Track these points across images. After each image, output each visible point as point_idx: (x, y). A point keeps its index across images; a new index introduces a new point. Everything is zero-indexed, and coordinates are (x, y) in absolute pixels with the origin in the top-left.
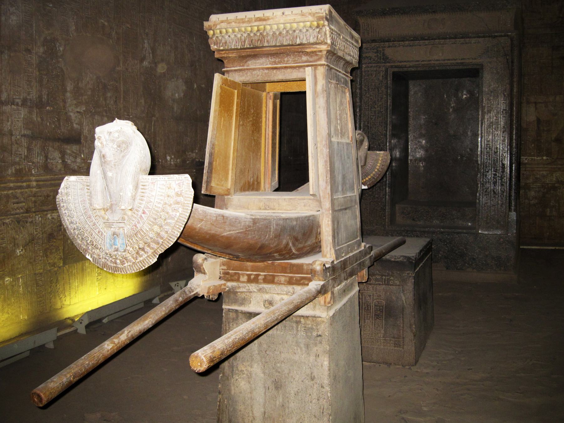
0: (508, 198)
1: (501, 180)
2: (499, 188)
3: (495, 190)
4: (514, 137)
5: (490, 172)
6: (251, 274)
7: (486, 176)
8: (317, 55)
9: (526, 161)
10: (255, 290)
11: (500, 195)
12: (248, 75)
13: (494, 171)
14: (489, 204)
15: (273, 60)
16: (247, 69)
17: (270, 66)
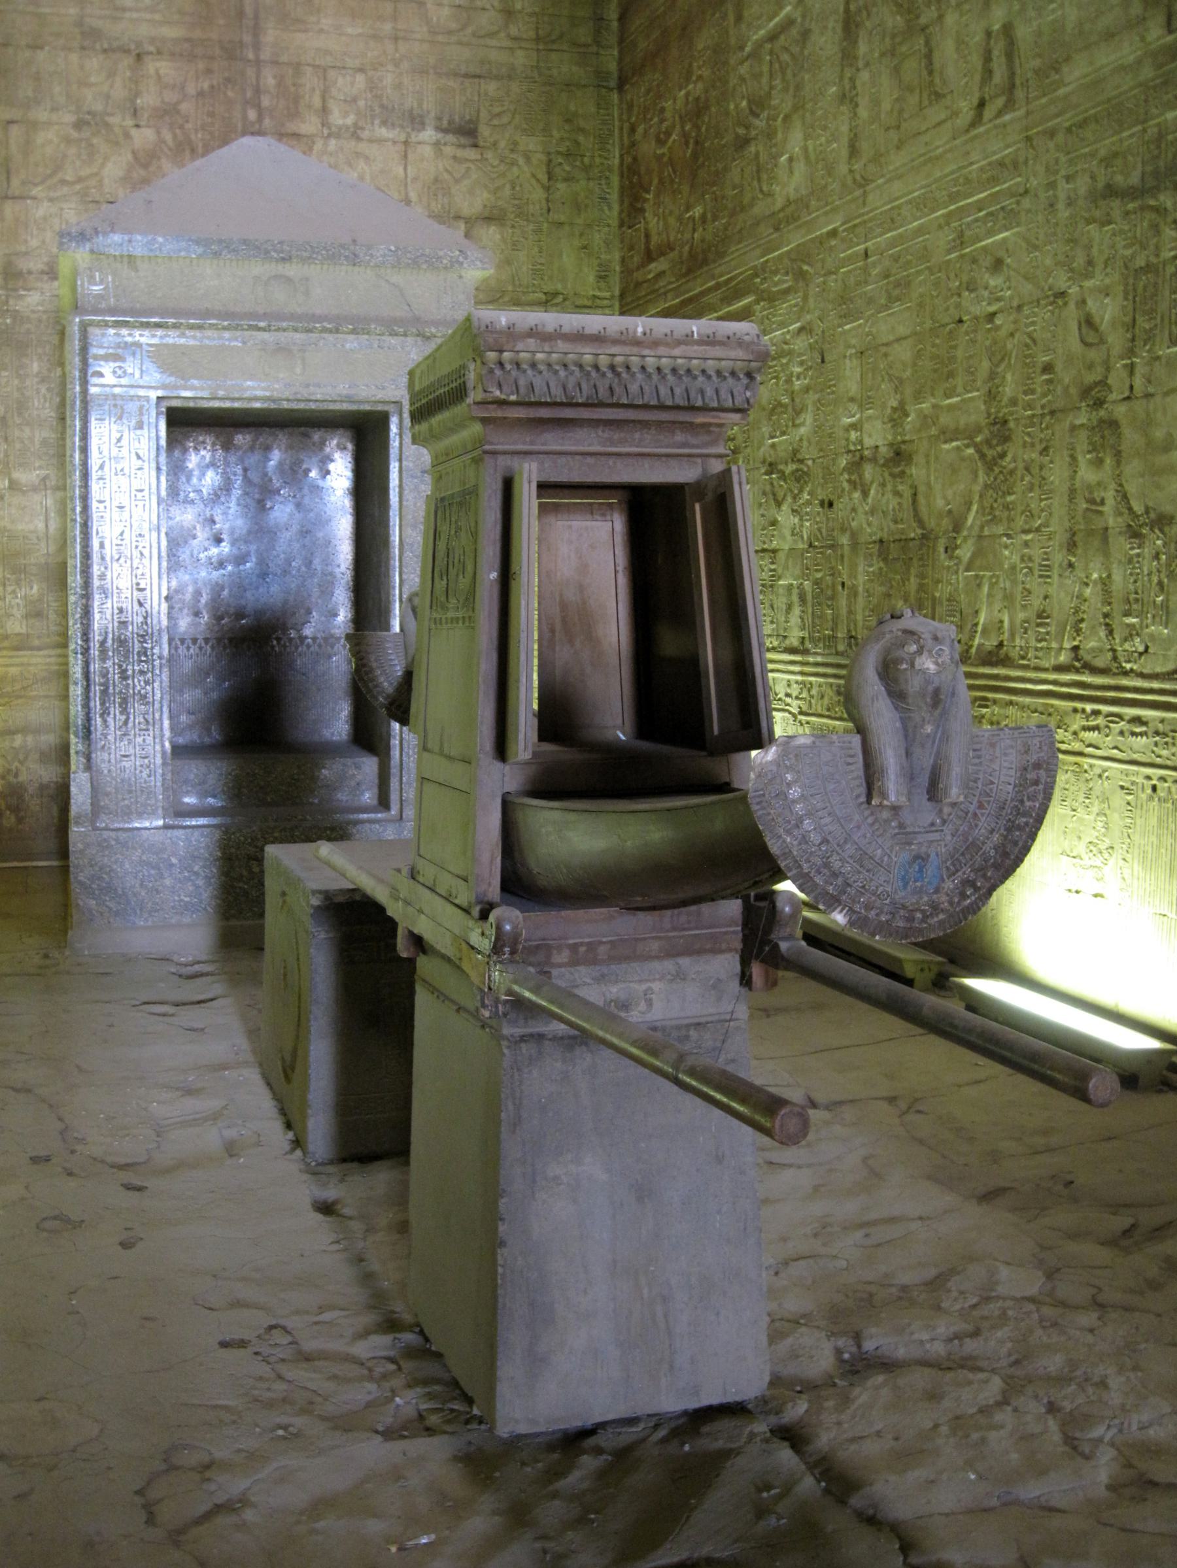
15: (606, 435)
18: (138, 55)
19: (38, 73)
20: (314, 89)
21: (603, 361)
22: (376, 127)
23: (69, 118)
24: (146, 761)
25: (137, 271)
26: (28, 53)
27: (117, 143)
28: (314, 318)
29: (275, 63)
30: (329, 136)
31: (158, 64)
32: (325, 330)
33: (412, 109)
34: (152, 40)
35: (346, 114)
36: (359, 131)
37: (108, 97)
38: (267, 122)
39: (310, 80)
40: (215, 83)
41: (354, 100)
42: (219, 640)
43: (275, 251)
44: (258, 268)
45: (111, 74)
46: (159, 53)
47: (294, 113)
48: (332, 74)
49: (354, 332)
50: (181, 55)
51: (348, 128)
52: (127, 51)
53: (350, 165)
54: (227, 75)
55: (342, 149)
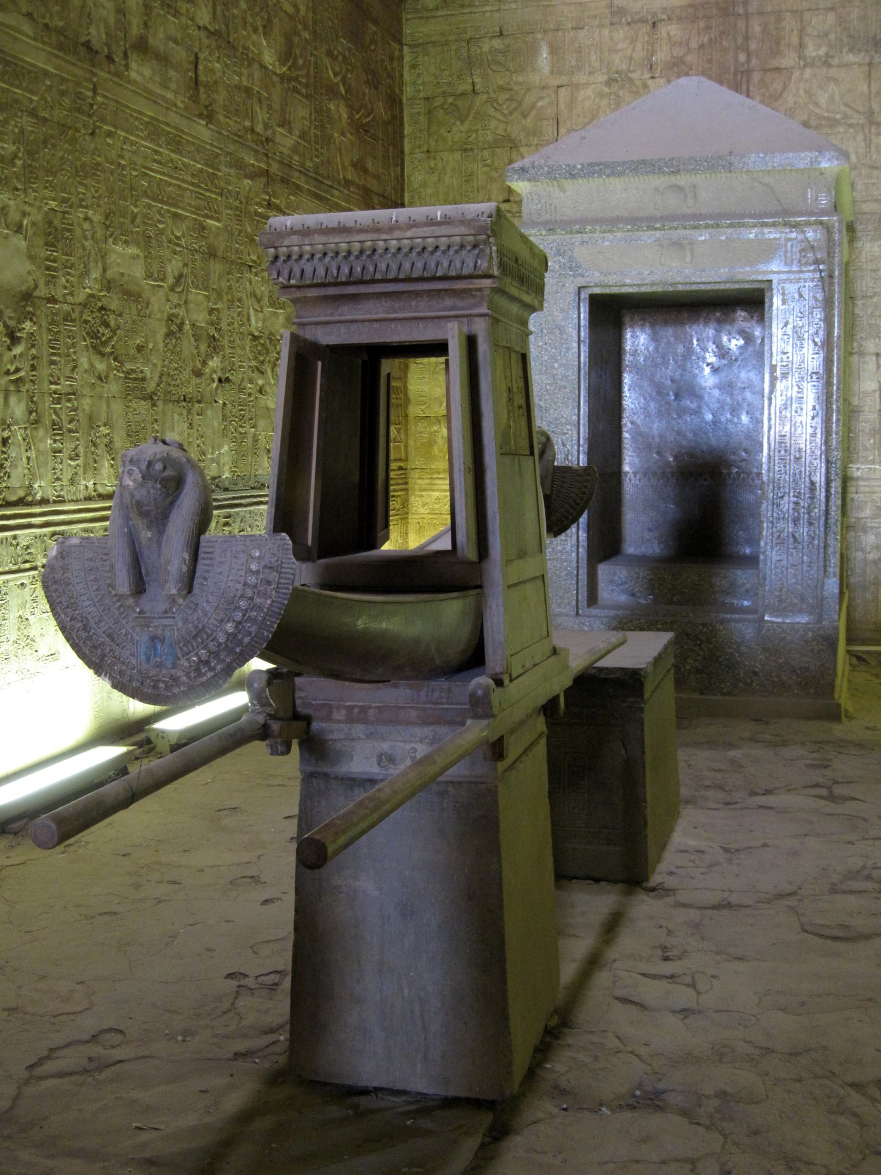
0: (821, 551)
1: (809, 513)
2: (803, 531)
3: (797, 535)
4: (834, 426)
5: (786, 498)
6: (355, 706)
7: (778, 505)
8: (473, 296)
9: (859, 474)
10: (363, 736)
11: (805, 544)
12: (342, 331)
13: (794, 496)
14: (784, 563)
15: (388, 305)
16: (340, 322)
17: (383, 316)
18: (654, 23)
19: (580, 47)
20: (792, 31)
21: (356, 246)
22: (845, 54)
23: (602, 78)
24: (565, 564)
25: (564, 192)
26: (572, 34)
27: (637, 93)
28: (701, 217)
29: (761, 13)
30: (805, 66)
31: (669, 28)
32: (707, 226)
33: (875, 35)
34: (664, 10)
35: (819, 47)
36: (829, 60)
37: (631, 58)
38: (754, 62)
39: (789, 23)
40: (713, 36)
41: (826, 35)
42: (664, 474)
43: (666, 166)
44: (656, 181)
45: (633, 41)
46: (669, 19)
47: (775, 52)
48: (807, 16)
49: (731, 226)
50: (686, 18)
51: (820, 58)
52: (646, 21)
53: (821, 87)
54: (722, 28)
55: (815, 76)
